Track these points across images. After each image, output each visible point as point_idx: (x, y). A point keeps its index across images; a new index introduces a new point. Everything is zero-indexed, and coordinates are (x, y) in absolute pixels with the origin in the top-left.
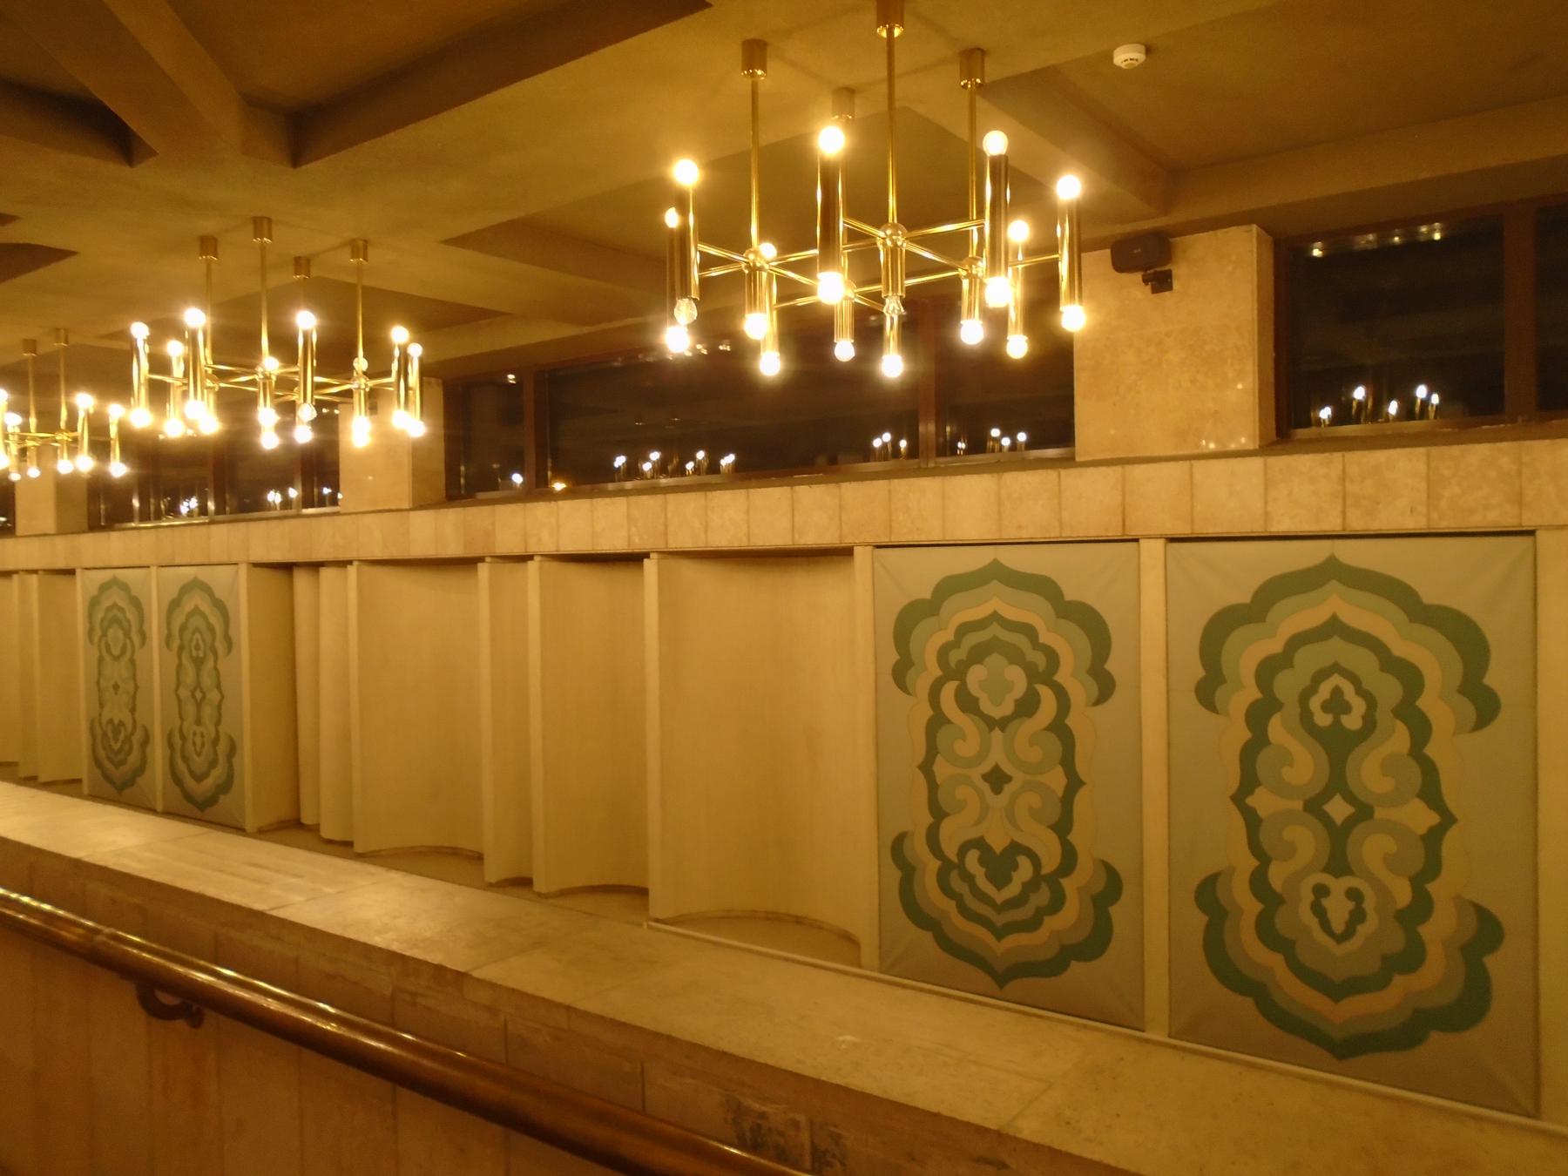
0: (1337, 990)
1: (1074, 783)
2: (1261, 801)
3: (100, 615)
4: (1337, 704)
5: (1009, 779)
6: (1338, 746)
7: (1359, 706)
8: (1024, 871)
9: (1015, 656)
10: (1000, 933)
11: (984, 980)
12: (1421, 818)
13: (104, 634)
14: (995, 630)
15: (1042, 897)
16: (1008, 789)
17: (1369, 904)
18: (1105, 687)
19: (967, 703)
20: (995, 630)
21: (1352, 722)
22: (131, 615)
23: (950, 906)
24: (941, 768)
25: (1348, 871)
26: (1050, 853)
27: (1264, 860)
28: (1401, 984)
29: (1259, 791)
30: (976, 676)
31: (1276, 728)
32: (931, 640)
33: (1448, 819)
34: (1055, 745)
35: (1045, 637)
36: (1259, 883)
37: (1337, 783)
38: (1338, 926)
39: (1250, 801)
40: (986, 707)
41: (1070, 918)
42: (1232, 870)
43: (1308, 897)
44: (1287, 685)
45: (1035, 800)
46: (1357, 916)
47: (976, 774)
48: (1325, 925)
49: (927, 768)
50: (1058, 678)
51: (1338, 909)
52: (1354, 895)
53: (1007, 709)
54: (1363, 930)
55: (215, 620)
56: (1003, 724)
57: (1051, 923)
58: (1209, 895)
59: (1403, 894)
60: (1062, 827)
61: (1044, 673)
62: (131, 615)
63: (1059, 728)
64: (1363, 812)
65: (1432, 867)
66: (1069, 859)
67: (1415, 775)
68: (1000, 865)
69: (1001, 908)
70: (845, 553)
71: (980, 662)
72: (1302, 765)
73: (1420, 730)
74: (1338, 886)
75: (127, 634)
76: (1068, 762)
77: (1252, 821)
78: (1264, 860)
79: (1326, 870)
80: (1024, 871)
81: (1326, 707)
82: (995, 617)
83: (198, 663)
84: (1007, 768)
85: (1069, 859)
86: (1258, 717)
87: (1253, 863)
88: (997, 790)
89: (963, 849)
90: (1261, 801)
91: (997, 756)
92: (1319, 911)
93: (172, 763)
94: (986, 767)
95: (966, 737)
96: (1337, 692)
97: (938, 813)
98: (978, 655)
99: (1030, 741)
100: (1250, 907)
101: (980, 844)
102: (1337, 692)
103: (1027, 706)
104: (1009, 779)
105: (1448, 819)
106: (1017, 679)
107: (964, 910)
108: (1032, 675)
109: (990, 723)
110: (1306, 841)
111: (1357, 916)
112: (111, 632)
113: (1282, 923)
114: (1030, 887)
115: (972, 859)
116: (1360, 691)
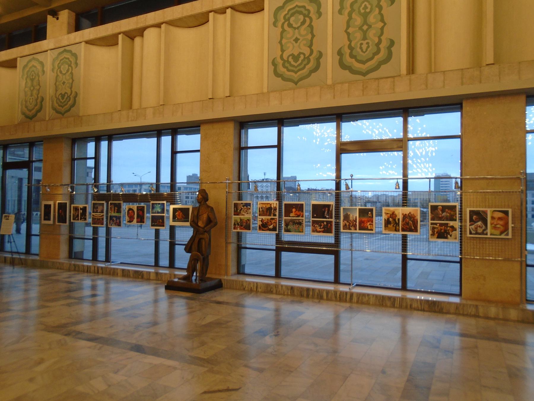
0: (363, 63)
1: (313, 36)
2: (350, 30)
4: (366, 7)
5: (299, 39)
6: (365, 16)
7: (369, 7)
8: (302, 57)
9: (300, 13)
10: (296, 73)
11: (291, 85)
14: (297, 9)
15: (305, 62)
16: (299, 41)
17: (370, 45)
18: (319, 14)
19: (290, 26)
20: (297, 9)
21: (368, 10)
23: (285, 70)
24: (284, 41)
25: (367, 39)
27: (350, 41)
28: (376, 57)
29: (350, 28)
30: (292, 20)
31: (354, 16)
33: (385, 24)
34: (309, 29)
35: (307, 7)
36: (350, 47)
37: (365, 22)
38: (364, 50)
39: (348, 31)
40: (294, 25)
41: (312, 65)
42: (344, 45)
43: (359, 46)
44: (356, 7)
45: (305, 42)
46: (368, 47)
47: (292, 40)
48: (362, 51)
49: (280, 42)
50: (310, 15)
51: (364, 47)
52: (368, 43)
53: (299, 24)
54: (369, 49)
56: (298, 28)
57: (307, 67)
58: (340, 53)
59: (376, 40)
60: (310, 46)
63: (311, 26)
64: (370, 27)
65: (382, 33)
66: (312, 52)
67: (379, 17)
68: (296, 58)
69: (296, 67)
71: (293, 16)
72: (358, 20)
73: (380, 8)
74: (364, 42)
76: (312, 32)
77: (348, 34)
78: (350, 41)
79: (362, 40)
80: (302, 57)
81: (363, 9)
82: (297, 6)
84: (299, 37)
85: (312, 52)
86: (350, 15)
87: (349, 43)
88: (296, 42)
89: (288, 58)
90: (350, 30)
91: (297, 35)
92: (361, 48)
93: (52, 104)
94: (294, 38)
96: (365, 5)
97: (283, 51)
98: (292, 15)
99: (303, 30)
100: (348, 51)
101: (292, 55)
102: (365, 5)
103: (303, 23)
104: (299, 39)
105: (385, 24)
106: (301, 17)
107: (288, 70)
108: (305, 16)
109: (295, 28)
110: (359, 35)
111: (368, 47)
113: (354, 53)
114: (303, 61)
115: (290, 59)
116: (370, 4)
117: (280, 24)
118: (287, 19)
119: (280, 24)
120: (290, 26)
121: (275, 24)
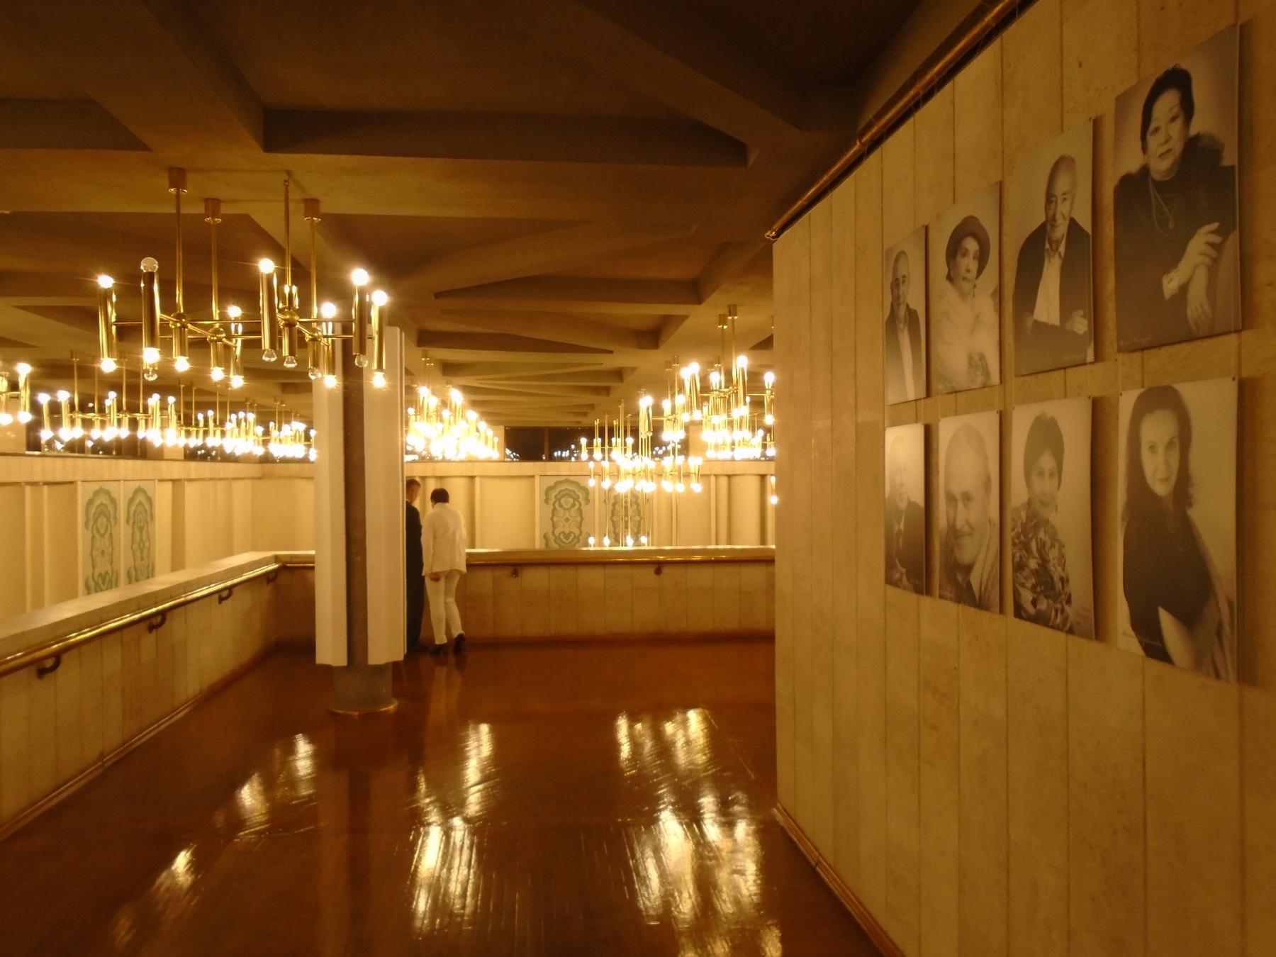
3: (133, 508)
12: (638, 518)
13: (96, 522)
18: (587, 501)
19: (561, 506)
22: (111, 509)
26: (577, 532)
32: (553, 494)
55: (147, 507)
60: (580, 527)
61: (576, 499)
62: (111, 509)
63: (579, 509)
68: (567, 536)
70: (533, 476)
75: (108, 520)
83: (141, 529)
91: (567, 515)
95: (561, 512)
97: (554, 527)
99: (573, 512)
103: (573, 505)
106: (571, 500)
112: (99, 521)
117: (551, 502)
118: (558, 499)
119: (551, 502)
120: (561, 506)
121: (546, 501)
